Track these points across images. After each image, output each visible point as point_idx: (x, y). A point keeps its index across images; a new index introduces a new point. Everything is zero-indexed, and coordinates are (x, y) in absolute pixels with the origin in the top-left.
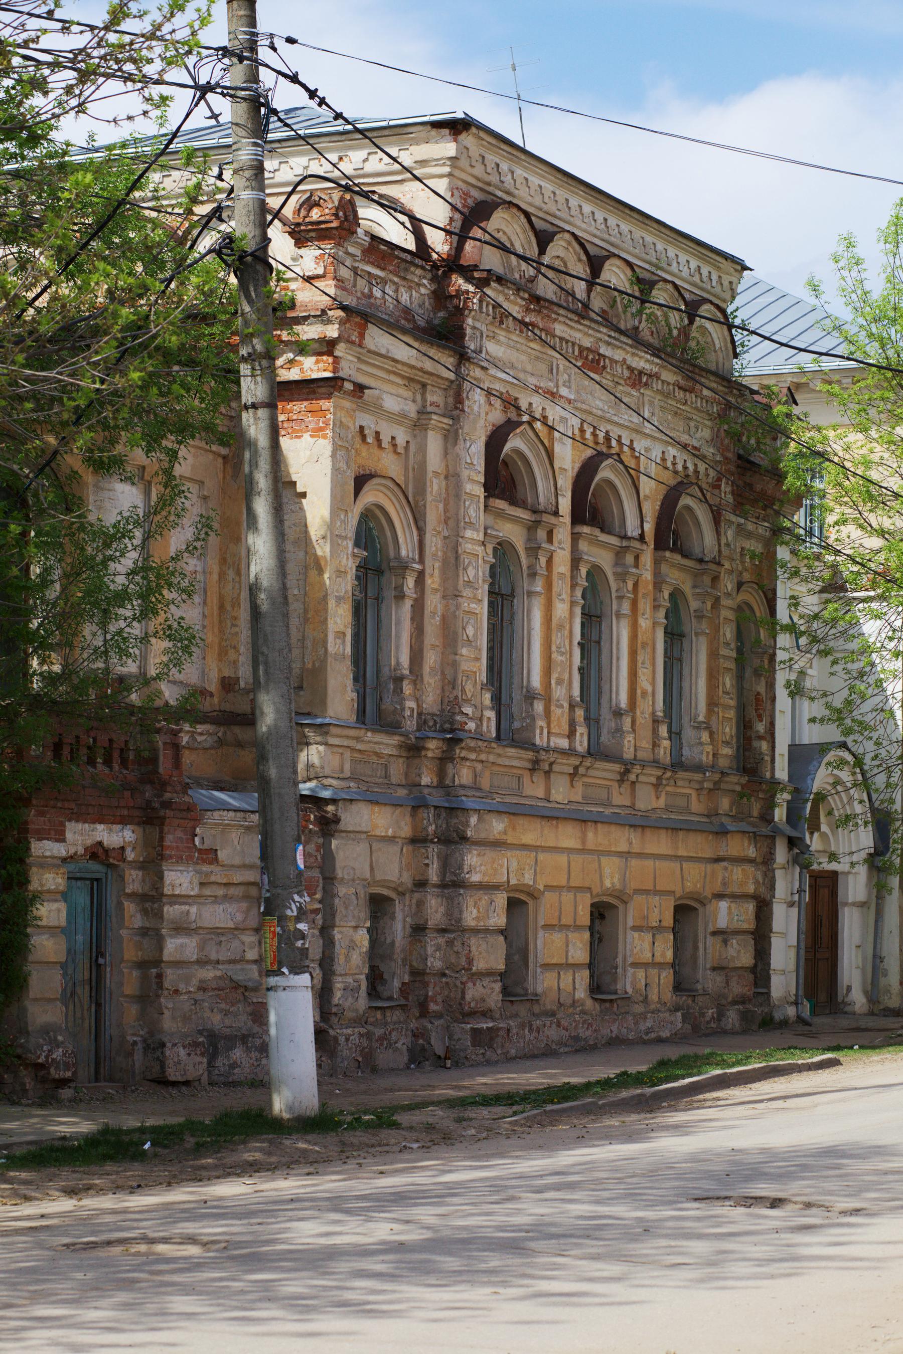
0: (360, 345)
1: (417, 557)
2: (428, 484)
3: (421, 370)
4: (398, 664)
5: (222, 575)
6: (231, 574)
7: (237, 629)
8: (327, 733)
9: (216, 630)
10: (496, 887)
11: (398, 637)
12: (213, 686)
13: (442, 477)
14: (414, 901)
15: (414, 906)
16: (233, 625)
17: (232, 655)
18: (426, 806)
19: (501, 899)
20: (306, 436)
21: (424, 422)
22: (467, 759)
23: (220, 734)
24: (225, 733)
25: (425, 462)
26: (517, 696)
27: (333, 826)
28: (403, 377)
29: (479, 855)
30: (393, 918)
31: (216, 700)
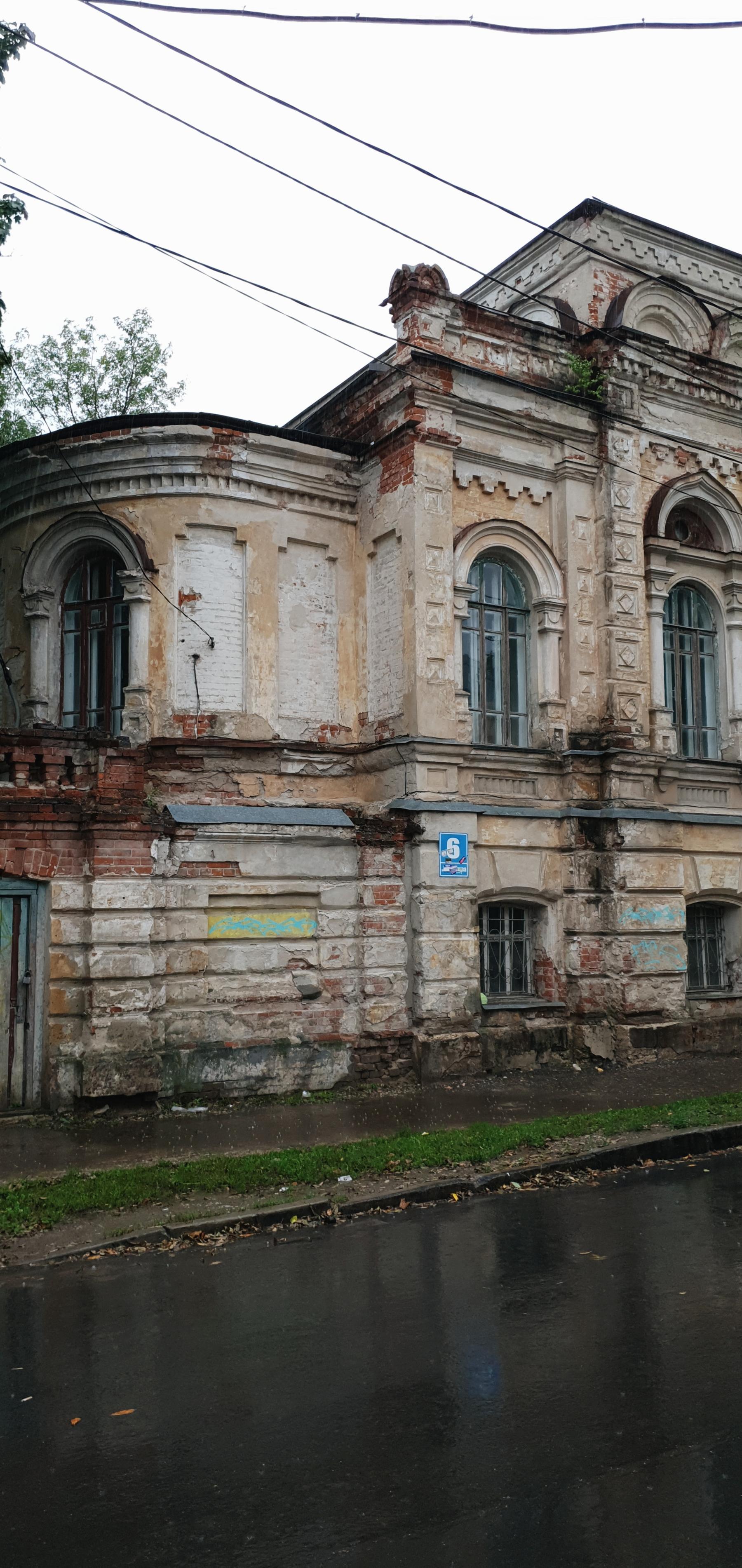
0: (447, 394)
1: (561, 594)
2: (570, 527)
3: (545, 422)
4: (545, 691)
5: (356, 625)
6: (361, 623)
7: (366, 671)
8: (414, 750)
9: (353, 674)
10: (677, 891)
11: (544, 666)
12: (351, 722)
13: (592, 521)
14: (565, 907)
15: (565, 911)
16: (364, 667)
17: (364, 694)
18: (569, 818)
19: (679, 904)
20: (401, 487)
21: (561, 472)
22: (629, 774)
23: (350, 763)
24: (355, 762)
25: (565, 508)
26: (723, 720)
27: (417, 838)
28: (530, 432)
29: (637, 861)
30: (546, 924)
31: (354, 734)
